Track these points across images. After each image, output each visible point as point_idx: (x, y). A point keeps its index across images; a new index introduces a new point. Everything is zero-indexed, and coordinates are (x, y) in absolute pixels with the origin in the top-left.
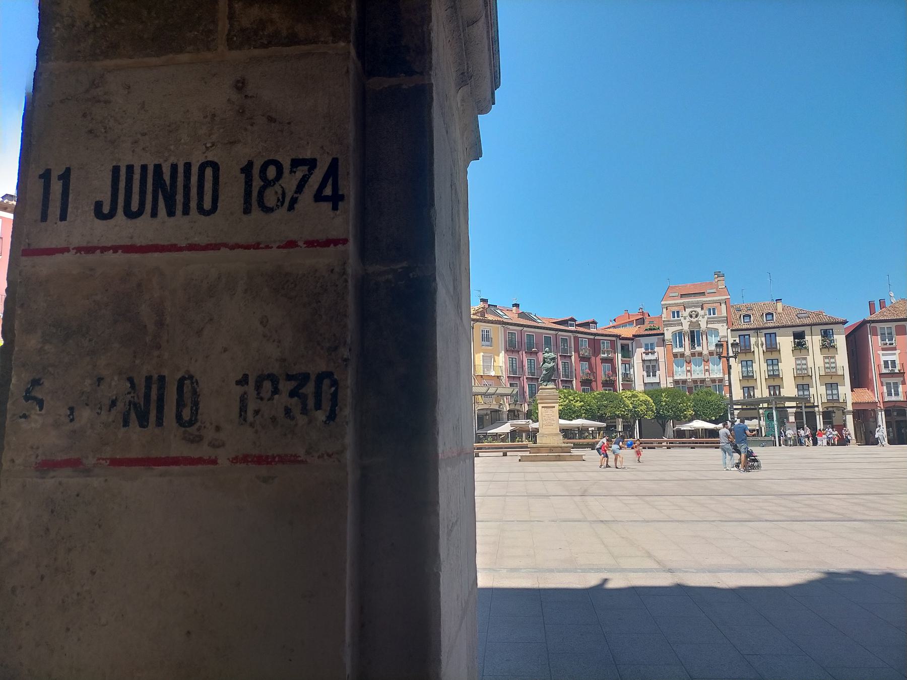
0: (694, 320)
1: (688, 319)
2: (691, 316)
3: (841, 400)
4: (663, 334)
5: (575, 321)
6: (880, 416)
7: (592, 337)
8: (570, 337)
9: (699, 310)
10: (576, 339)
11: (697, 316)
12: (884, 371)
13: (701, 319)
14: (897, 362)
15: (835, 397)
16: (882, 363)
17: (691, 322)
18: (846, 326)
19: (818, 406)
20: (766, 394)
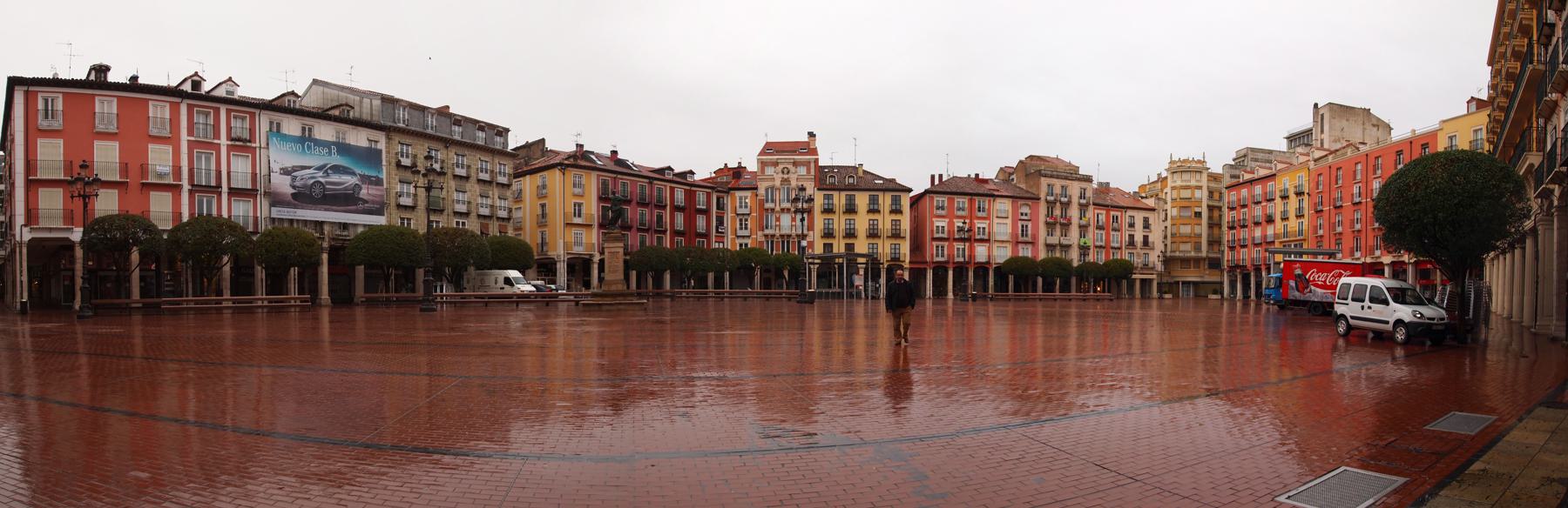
0: (786, 176)
1: (781, 175)
2: (783, 172)
3: (901, 259)
4: (756, 189)
5: (672, 170)
6: (928, 274)
7: (688, 188)
8: (665, 186)
9: (790, 167)
10: (672, 189)
11: (788, 172)
12: (936, 236)
13: (791, 175)
14: (946, 229)
15: (897, 256)
16: (935, 228)
17: (783, 178)
18: (912, 194)
19: (883, 264)
20: (843, 250)
